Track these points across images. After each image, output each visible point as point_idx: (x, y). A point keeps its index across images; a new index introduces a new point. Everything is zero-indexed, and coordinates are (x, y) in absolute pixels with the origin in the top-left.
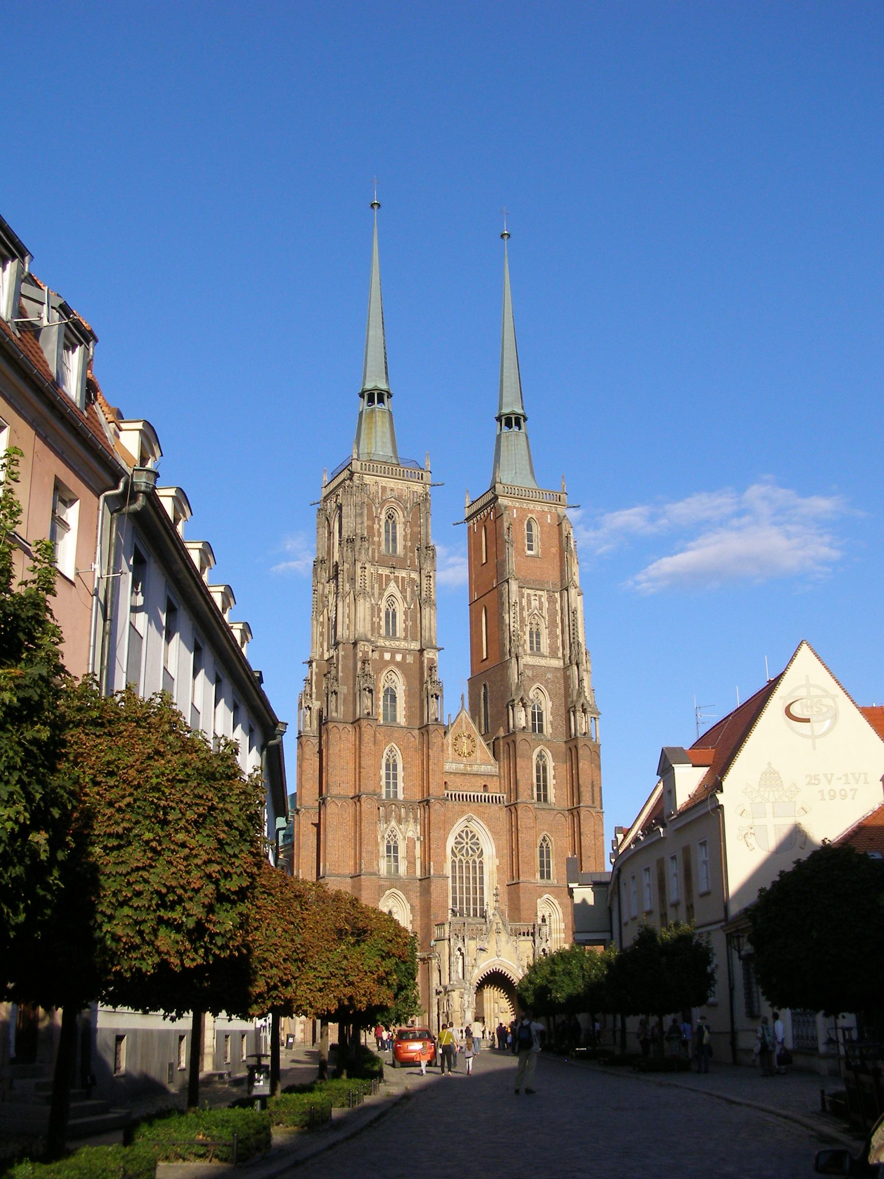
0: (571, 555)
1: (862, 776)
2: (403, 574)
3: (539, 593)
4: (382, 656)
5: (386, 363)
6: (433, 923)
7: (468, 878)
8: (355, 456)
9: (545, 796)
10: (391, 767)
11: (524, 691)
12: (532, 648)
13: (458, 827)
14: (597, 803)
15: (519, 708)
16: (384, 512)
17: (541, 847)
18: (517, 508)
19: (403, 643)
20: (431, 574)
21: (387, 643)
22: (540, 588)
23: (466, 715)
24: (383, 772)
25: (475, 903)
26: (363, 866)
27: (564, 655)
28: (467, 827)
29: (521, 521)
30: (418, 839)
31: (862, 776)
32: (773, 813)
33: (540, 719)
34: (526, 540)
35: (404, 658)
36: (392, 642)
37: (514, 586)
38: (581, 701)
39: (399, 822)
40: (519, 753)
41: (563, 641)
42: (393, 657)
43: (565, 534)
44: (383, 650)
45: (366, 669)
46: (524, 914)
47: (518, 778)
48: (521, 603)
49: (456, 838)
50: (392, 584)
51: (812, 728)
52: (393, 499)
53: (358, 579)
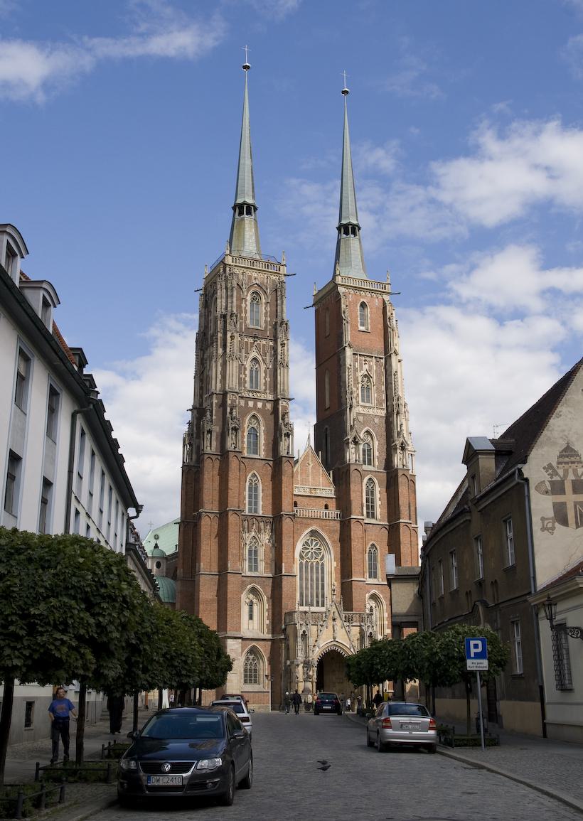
3: (368, 359)
4: (247, 404)
5: (253, 184)
8: (228, 252)
9: (373, 514)
10: (253, 489)
12: (363, 401)
15: (352, 445)
16: (249, 295)
20: (285, 342)
21: (251, 394)
24: (247, 493)
25: (317, 596)
26: (229, 565)
29: (355, 304)
33: (369, 455)
34: (359, 319)
35: (264, 406)
37: (349, 352)
42: (255, 405)
43: (389, 314)
45: (234, 413)
46: (355, 606)
48: (354, 366)
49: (304, 545)
50: (254, 349)
53: (228, 344)
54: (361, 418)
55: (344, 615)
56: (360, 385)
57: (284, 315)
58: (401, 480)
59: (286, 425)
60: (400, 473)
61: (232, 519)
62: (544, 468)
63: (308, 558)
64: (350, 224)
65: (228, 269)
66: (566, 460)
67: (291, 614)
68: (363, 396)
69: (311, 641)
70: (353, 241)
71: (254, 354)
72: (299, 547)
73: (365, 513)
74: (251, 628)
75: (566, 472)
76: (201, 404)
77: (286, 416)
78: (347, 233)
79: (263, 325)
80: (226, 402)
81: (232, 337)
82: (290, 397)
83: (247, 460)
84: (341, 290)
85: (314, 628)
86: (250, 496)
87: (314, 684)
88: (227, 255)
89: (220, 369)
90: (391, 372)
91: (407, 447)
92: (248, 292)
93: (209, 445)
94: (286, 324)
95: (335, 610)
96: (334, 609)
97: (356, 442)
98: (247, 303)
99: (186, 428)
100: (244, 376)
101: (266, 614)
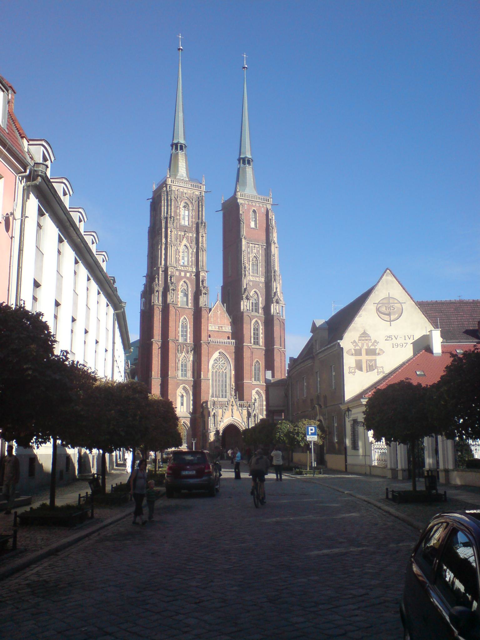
0: (273, 228)
2: (191, 235)
3: (257, 246)
4: (180, 274)
7: (219, 380)
9: (257, 342)
11: (248, 292)
12: (253, 273)
13: (216, 355)
17: (255, 365)
18: (247, 204)
19: (190, 268)
21: (183, 268)
22: (258, 244)
23: (219, 303)
24: (180, 329)
26: (169, 373)
28: (219, 356)
29: (249, 210)
35: (191, 275)
36: (185, 267)
37: (244, 242)
38: (276, 298)
39: (188, 352)
40: (245, 321)
42: (186, 274)
43: (270, 217)
44: (180, 271)
45: (172, 280)
46: (245, 397)
48: (247, 250)
49: (214, 361)
52: (186, 198)
53: (169, 236)
54: (251, 284)
55: (238, 404)
56: (251, 263)
57: (204, 217)
58: (276, 322)
59: (204, 287)
61: (171, 345)
62: (351, 343)
63: (217, 369)
64: (246, 157)
65: (168, 187)
66: (363, 338)
67: (206, 402)
68: (253, 269)
69: (219, 419)
70: (249, 170)
71: (185, 242)
72: (211, 362)
73: (252, 342)
74: (182, 410)
75: (363, 345)
76: (152, 272)
78: (244, 163)
79: (191, 224)
80: (168, 272)
83: (180, 309)
85: (220, 411)
86: (182, 331)
88: (168, 178)
89: (163, 252)
90: (271, 255)
91: (280, 302)
92: (181, 202)
93: (157, 299)
94: (205, 223)
95: (233, 400)
96: (233, 399)
97: (248, 299)
100: (178, 256)
101: (191, 402)
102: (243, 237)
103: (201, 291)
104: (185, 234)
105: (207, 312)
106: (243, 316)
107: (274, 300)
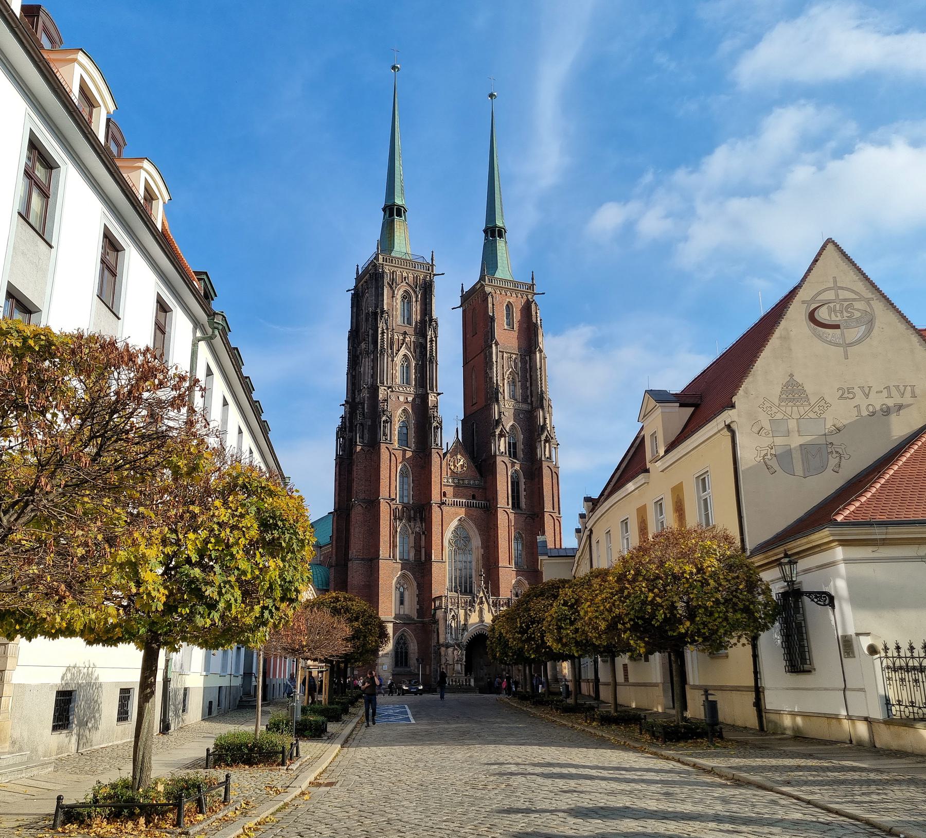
1: (909, 388)
6: (433, 597)
11: (503, 425)
14: (556, 510)
20: (434, 339)
21: (401, 389)
26: (381, 553)
27: (532, 401)
30: (424, 533)
31: (909, 388)
32: (799, 431)
33: (515, 448)
40: (498, 470)
41: (531, 391)
47: (498, 489)
51: (843, 334)
55: (491, 601)
60: (545, 464)
71: (403, 351)
76: (354, 399)
77: (435, 410)
80: (378, 396)
81: (383, 333)
82: (438, 391)
84: (488, 289)
87: (463, 666)
98: (397, 301)
99: (339, 422)
102: (494, 342)
103: (431, 424)
104: (405, 338)
105: (440, 455)
106: (495, 462)
107: (543, 437)
